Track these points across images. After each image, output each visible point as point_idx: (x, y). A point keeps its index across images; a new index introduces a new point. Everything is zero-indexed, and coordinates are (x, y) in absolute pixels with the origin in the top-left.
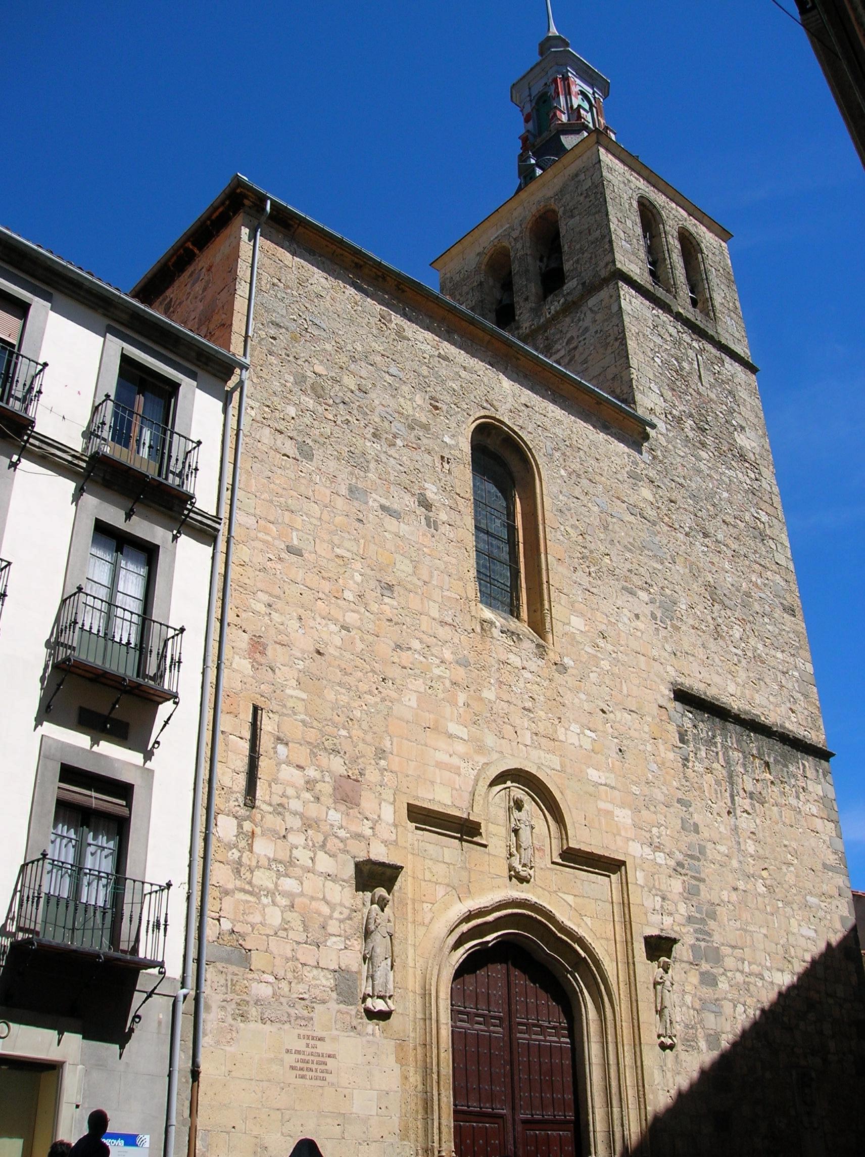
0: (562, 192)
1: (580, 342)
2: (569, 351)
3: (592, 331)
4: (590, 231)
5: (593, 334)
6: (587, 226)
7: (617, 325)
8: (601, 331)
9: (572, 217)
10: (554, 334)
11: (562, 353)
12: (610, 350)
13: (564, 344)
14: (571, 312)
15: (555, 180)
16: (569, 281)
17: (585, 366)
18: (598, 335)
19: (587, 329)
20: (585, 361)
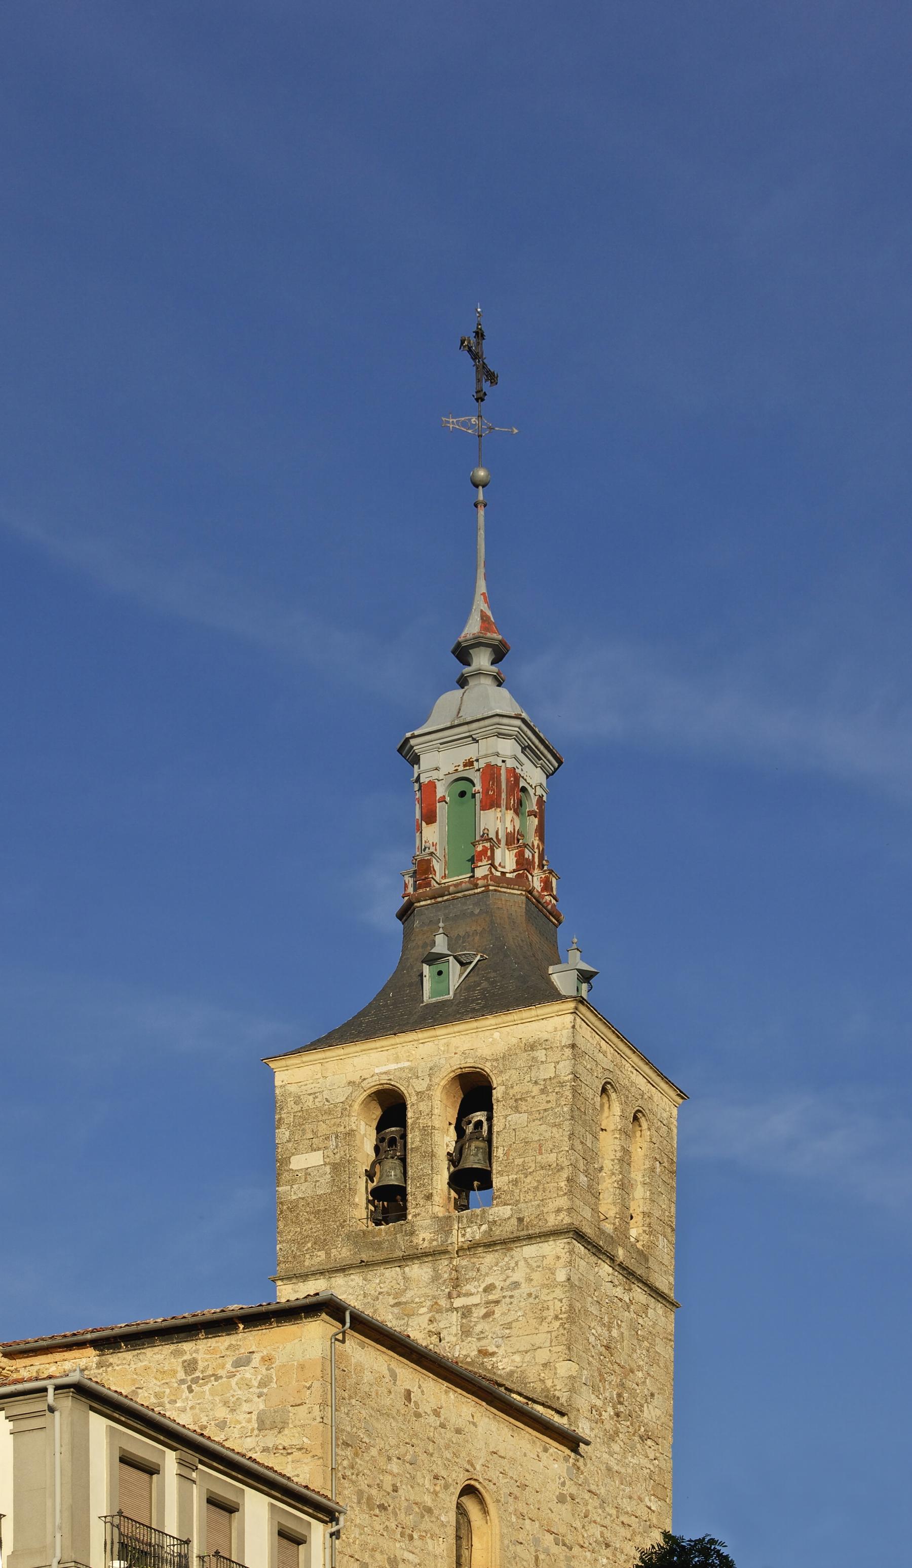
0: (506, 1058)
1: (504, 1297)
2: (488, 1303)
3: (525, 1289)
4: (540, 1146)
5: (525, 1295)
6: (536, 1138)
7: (561, 1301)
8: (536, 1297)
9: (516, 1109)
10: (466, 1267)
11: (475, 1300)
12: (545, 1327)
13: (481, 1289)
14: (496, 1251)
15: (496, 1035)
16: (497, 1205)
17: (508, 1331)
18: (531, 1300)
19: (516, 1285)
20: (509, 1326)
